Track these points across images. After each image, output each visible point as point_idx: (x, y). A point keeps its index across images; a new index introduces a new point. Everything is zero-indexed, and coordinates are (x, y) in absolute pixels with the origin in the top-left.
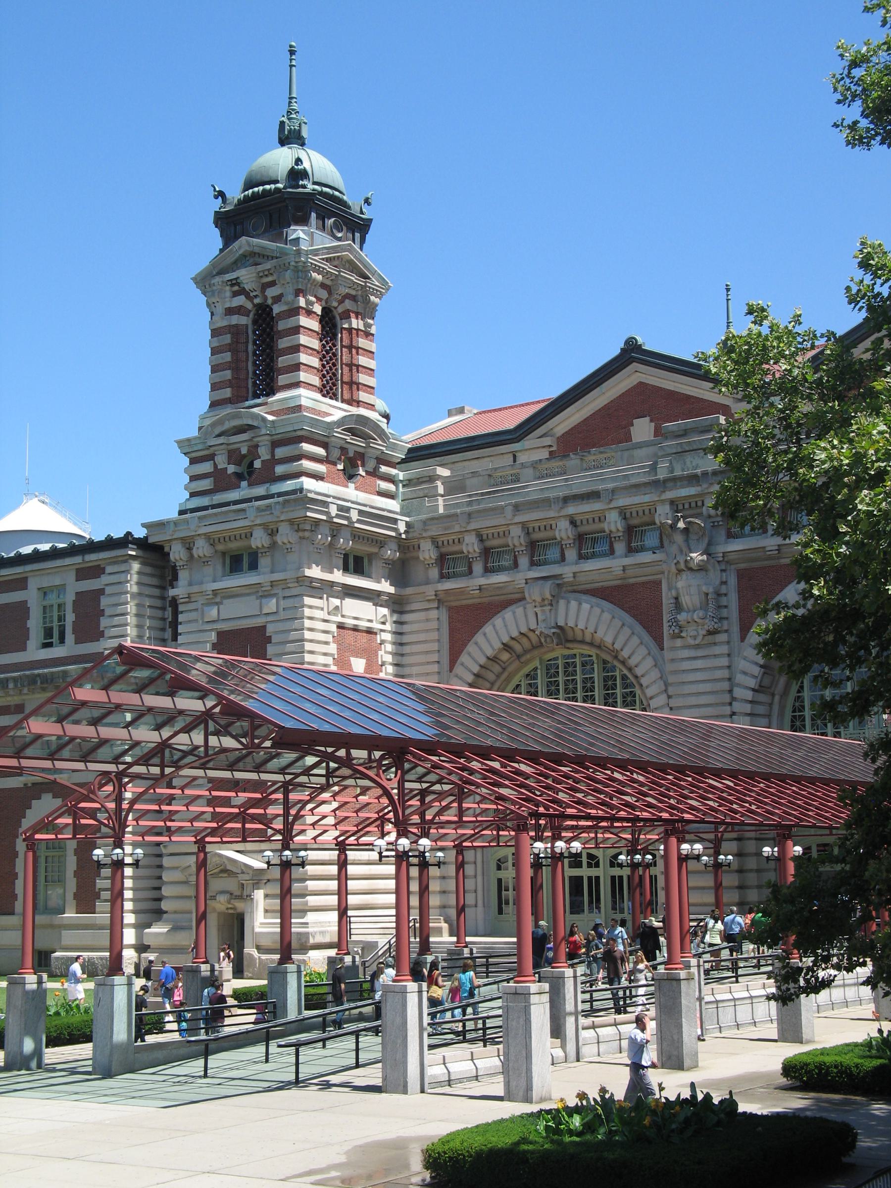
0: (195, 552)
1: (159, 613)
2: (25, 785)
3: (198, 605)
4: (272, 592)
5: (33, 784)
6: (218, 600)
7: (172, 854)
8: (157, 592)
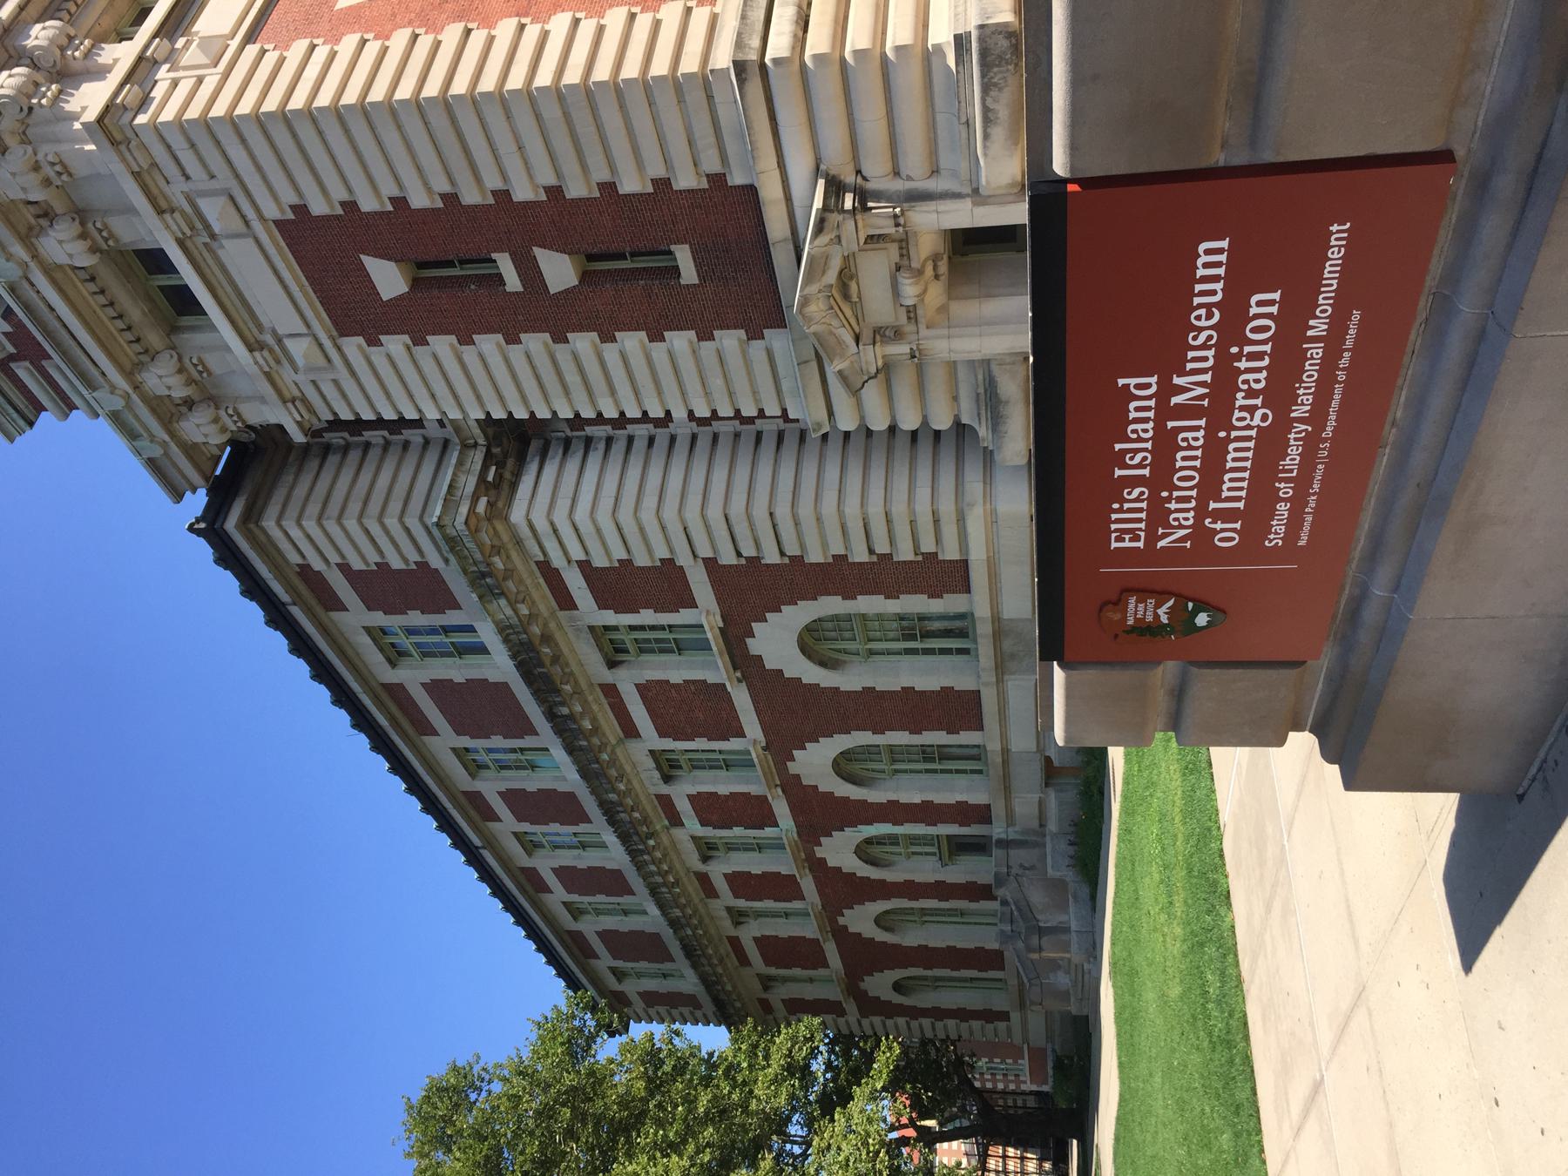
0: (179, 393)
1: (374, 454)
2: (739, 681)
3: (301, 378)
4: (188, 209)
5: (735, 669)
6: (269, 339)
7: (831, 414)
8: (333, 459)
